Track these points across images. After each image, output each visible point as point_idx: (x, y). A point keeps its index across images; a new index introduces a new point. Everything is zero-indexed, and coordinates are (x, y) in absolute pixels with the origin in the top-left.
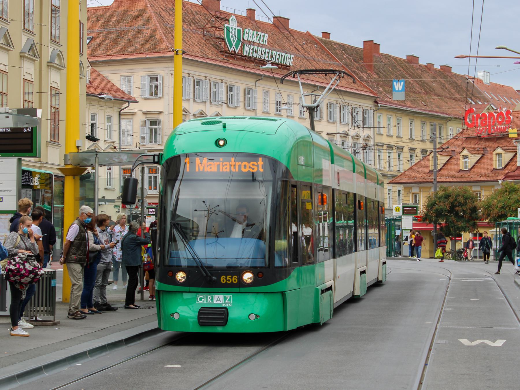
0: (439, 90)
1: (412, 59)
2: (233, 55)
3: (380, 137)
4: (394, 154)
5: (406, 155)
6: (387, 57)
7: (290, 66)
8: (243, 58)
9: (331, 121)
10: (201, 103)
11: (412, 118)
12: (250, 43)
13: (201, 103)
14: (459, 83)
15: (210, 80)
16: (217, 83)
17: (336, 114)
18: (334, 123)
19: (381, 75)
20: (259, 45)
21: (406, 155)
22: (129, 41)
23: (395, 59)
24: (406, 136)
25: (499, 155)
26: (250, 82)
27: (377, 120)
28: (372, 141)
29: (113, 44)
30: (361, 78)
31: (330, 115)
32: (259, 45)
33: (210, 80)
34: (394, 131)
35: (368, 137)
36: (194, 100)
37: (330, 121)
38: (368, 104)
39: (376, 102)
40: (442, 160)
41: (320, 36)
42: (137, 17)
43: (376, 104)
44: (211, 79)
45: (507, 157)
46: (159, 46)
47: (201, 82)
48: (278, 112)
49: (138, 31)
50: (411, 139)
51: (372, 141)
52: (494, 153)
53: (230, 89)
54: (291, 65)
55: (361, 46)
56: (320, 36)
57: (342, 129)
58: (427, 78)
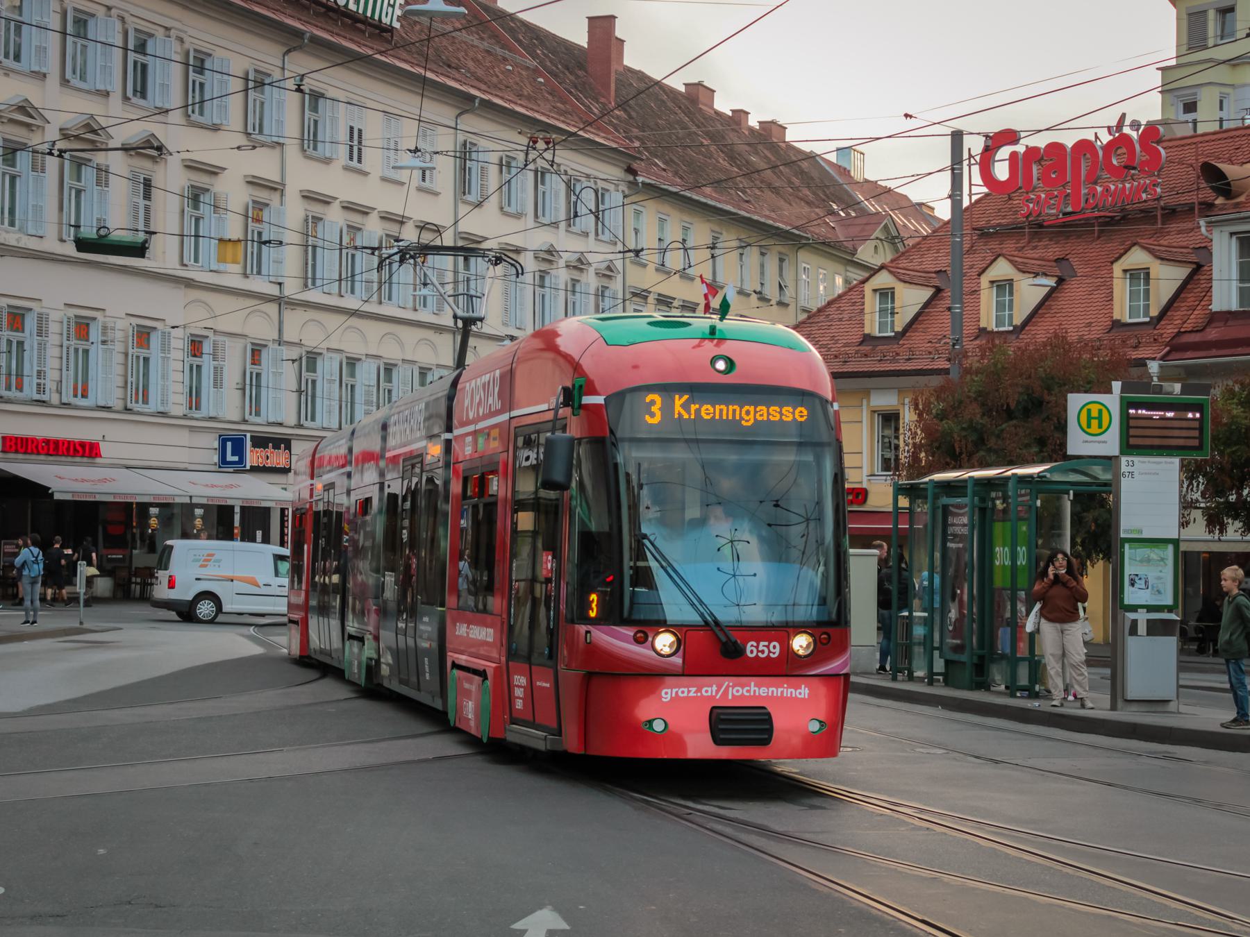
3: (640, 268)
7: (390, 29)
9: (512, 210)
10: (88, 92)
11: (717, 228)
13: (88, 92)
15: (122, 19)
16: (151, 35)
17: (523, 190)
18: (518, 216)
19: (634, 114)
25: (1139, 276)
26: (263, 53)
27: (630, 224)
28: (620, 278)
33: (122, 19)
35: (609, 268)
36: (65, 82)
37: (506, 209)
39: (631, 171)
40: (911, 299)
43: (631, 178)
44: (129, 19)
45: (1167, 278)
47: (91, 23)
48: (355, 163)
51: (620, 278)
52: (1117, 269)
54: (397, 25)
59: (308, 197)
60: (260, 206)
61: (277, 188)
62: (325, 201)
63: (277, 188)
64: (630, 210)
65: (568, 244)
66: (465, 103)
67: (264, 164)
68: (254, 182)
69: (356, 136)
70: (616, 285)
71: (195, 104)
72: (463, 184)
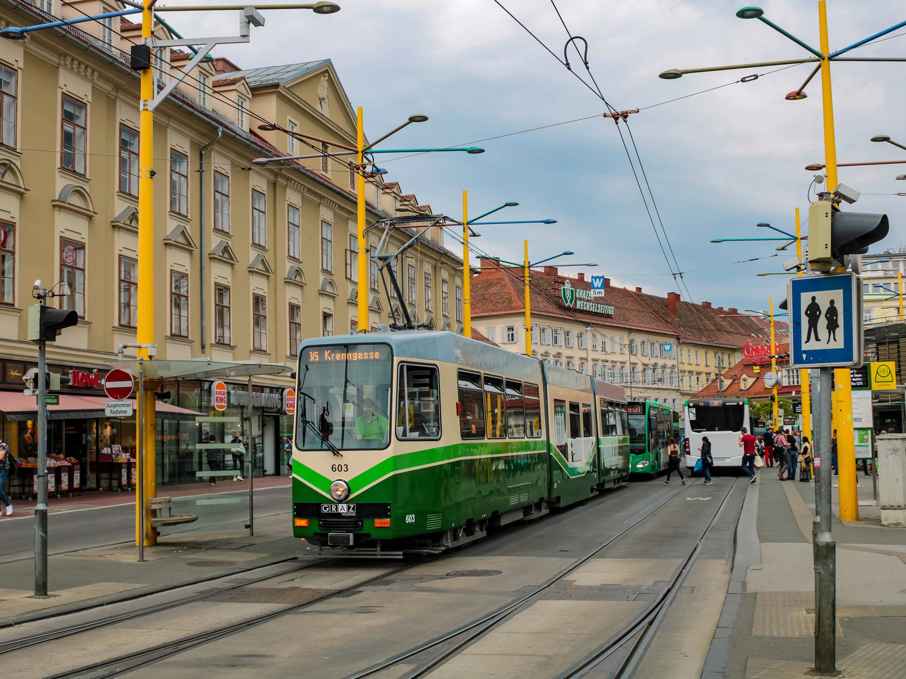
0: (728, 328)
1: (707, 305)
2: (568, 309)
4: (694, 377)
5: (703, 377)
6: (686, 303)
8: (575, 310)
12: (581, 299)
14: (744, 321)
20: (588, 301)
21: (703, 377)
22: (491, 301)
23: (693, 305)
24: (703, 364)
29: (480, 304)
30: (667, 322)
31: (643, 350)
32: (588, 301)
34: (693, 361)
38: (673, 341)
39: (678, 339)
40: (727, 382)
41: (634, 290)
42: (497, 284)
46: (513, 305)
49: (498, 294)
50: (707, 366)
53: (568, 333)
55: (666, 297)
56: (634, 290)
57: (653, 361)
58: (718, 318)
59: (593, 360)
60: (582, 364)
61: (586, 359)
62: (597, 360)
63: (586, 359)
64: (679, 349)
65: (661, 362)
66: (631, 331)
67: (583, 354)
68: (581, 359)
69: (604, 343)
70: (676, 370)
71: (567, 341)
72: (631, 352)
